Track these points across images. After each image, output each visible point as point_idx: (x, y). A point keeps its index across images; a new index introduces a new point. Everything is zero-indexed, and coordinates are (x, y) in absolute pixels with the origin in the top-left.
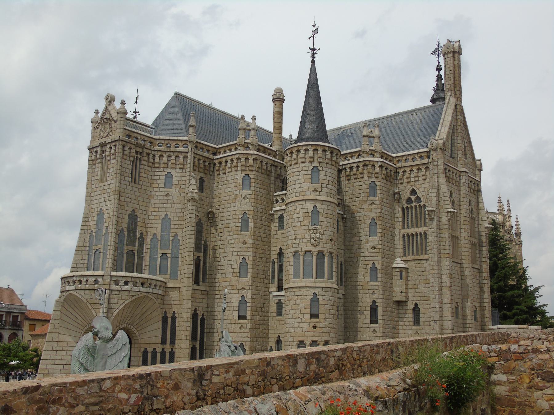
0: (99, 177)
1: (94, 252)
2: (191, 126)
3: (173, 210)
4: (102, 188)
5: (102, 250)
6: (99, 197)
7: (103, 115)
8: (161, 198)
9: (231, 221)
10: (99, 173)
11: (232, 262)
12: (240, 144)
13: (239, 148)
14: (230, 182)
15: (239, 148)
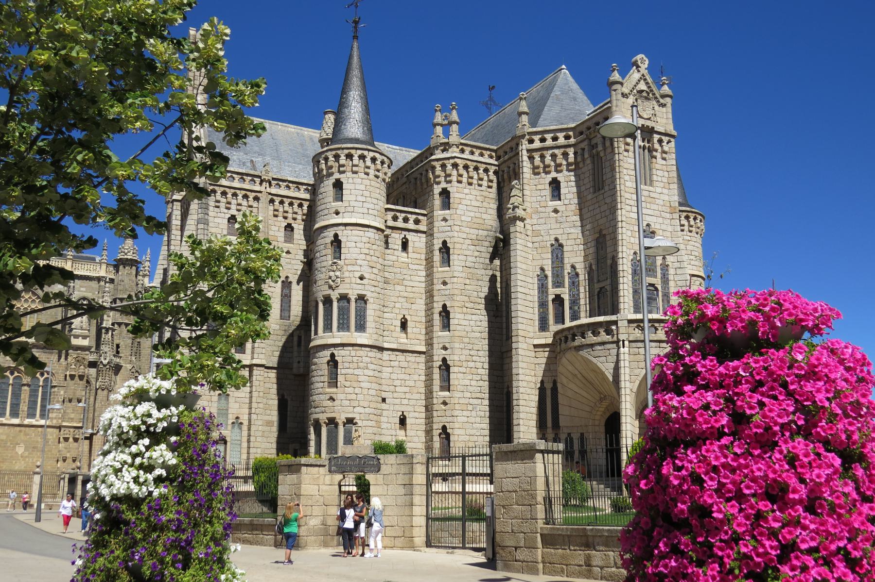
5: (659, 288)
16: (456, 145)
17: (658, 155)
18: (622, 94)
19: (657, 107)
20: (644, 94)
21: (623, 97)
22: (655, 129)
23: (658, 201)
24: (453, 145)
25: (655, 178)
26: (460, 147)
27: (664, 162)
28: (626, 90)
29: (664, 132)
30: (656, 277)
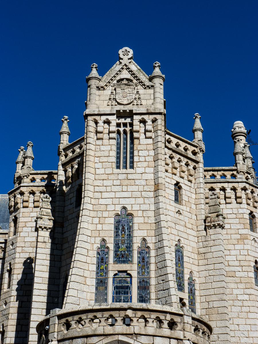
0: (114, 160)
1: (111, 274)
2: (199, 130)
3: (185, 235)
4: (121, 177)
5: (134, 274)
6: (119, 188)
7: (117, 74)
8: (171, 213)
9: (240, 269)
10: (114, 153)
11: (248, 328)
12: (241, 172)
13: (239, 176)
14: (229, 216)
15: (239, 176)
16: (26, 176)
17: (142, 136)
18: (97, 87)
19: (142, 91)
20: (125, 82)
21: (99, 89)
22: (134, 112)
23: (137, 182)
24: (24, 176)
25: (136, 159)
26: (31, 177)
27: (150, 141)
28: (102, 84)
29: (145, 112)
30: (131, 262)
